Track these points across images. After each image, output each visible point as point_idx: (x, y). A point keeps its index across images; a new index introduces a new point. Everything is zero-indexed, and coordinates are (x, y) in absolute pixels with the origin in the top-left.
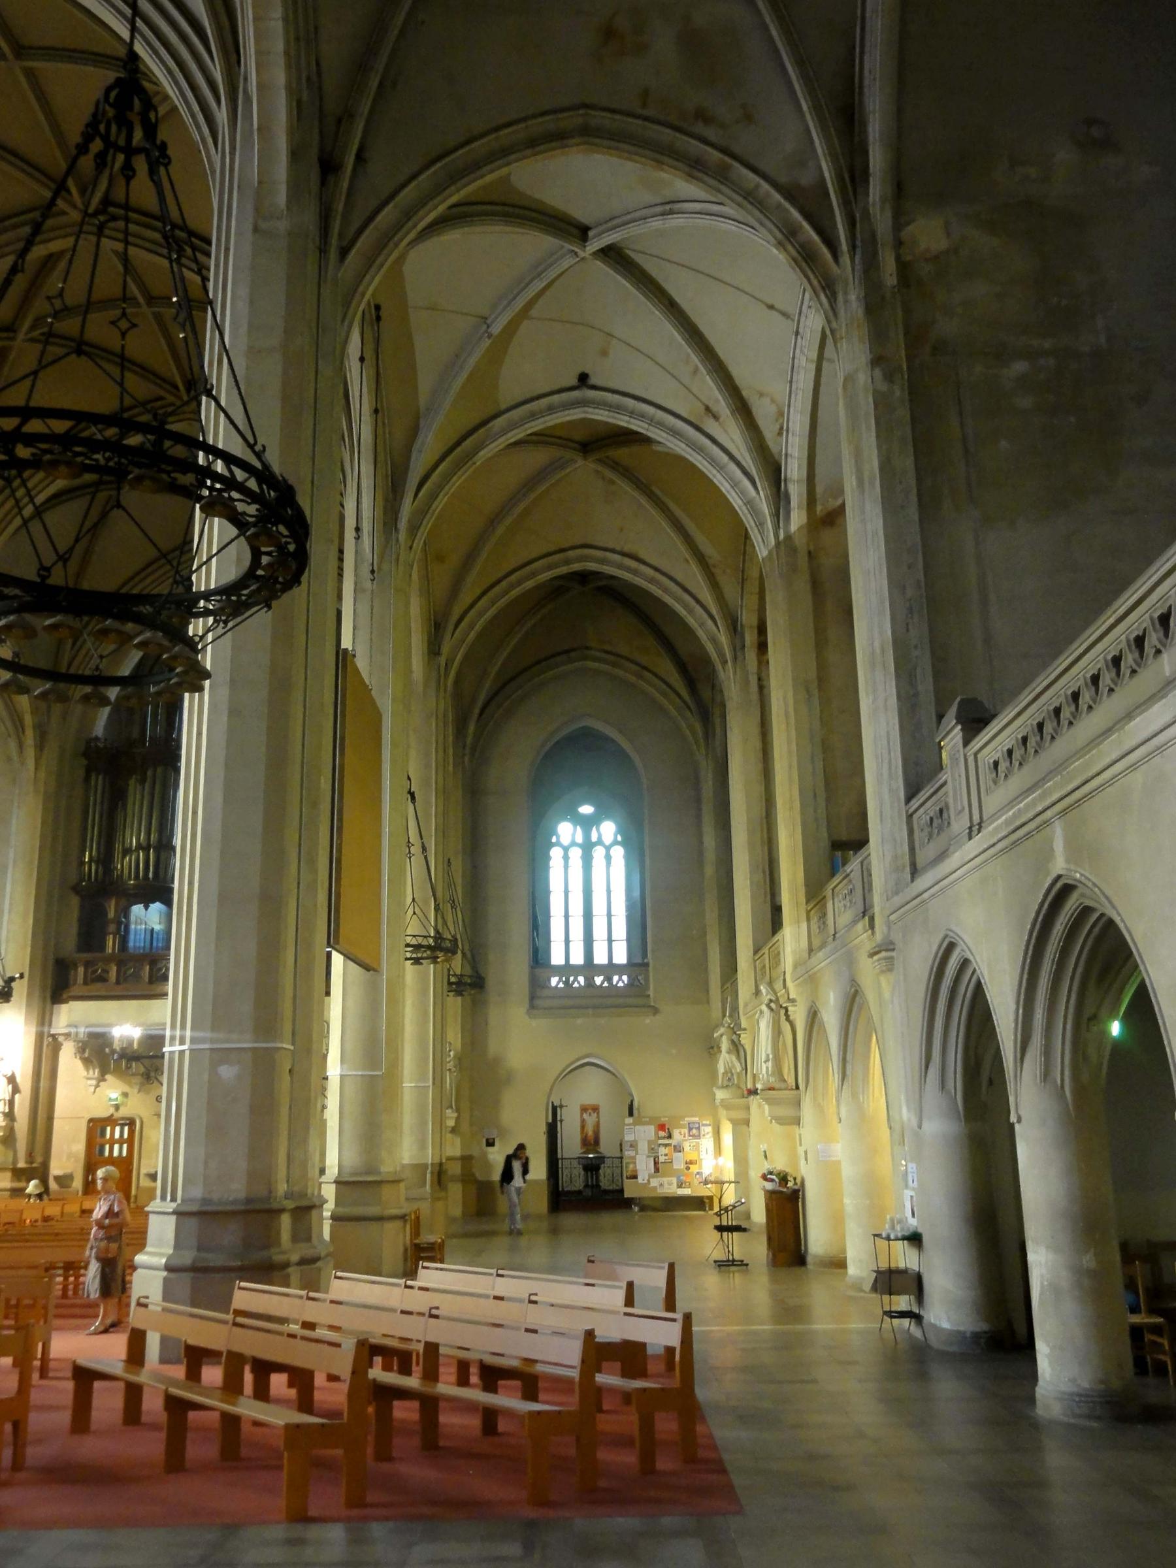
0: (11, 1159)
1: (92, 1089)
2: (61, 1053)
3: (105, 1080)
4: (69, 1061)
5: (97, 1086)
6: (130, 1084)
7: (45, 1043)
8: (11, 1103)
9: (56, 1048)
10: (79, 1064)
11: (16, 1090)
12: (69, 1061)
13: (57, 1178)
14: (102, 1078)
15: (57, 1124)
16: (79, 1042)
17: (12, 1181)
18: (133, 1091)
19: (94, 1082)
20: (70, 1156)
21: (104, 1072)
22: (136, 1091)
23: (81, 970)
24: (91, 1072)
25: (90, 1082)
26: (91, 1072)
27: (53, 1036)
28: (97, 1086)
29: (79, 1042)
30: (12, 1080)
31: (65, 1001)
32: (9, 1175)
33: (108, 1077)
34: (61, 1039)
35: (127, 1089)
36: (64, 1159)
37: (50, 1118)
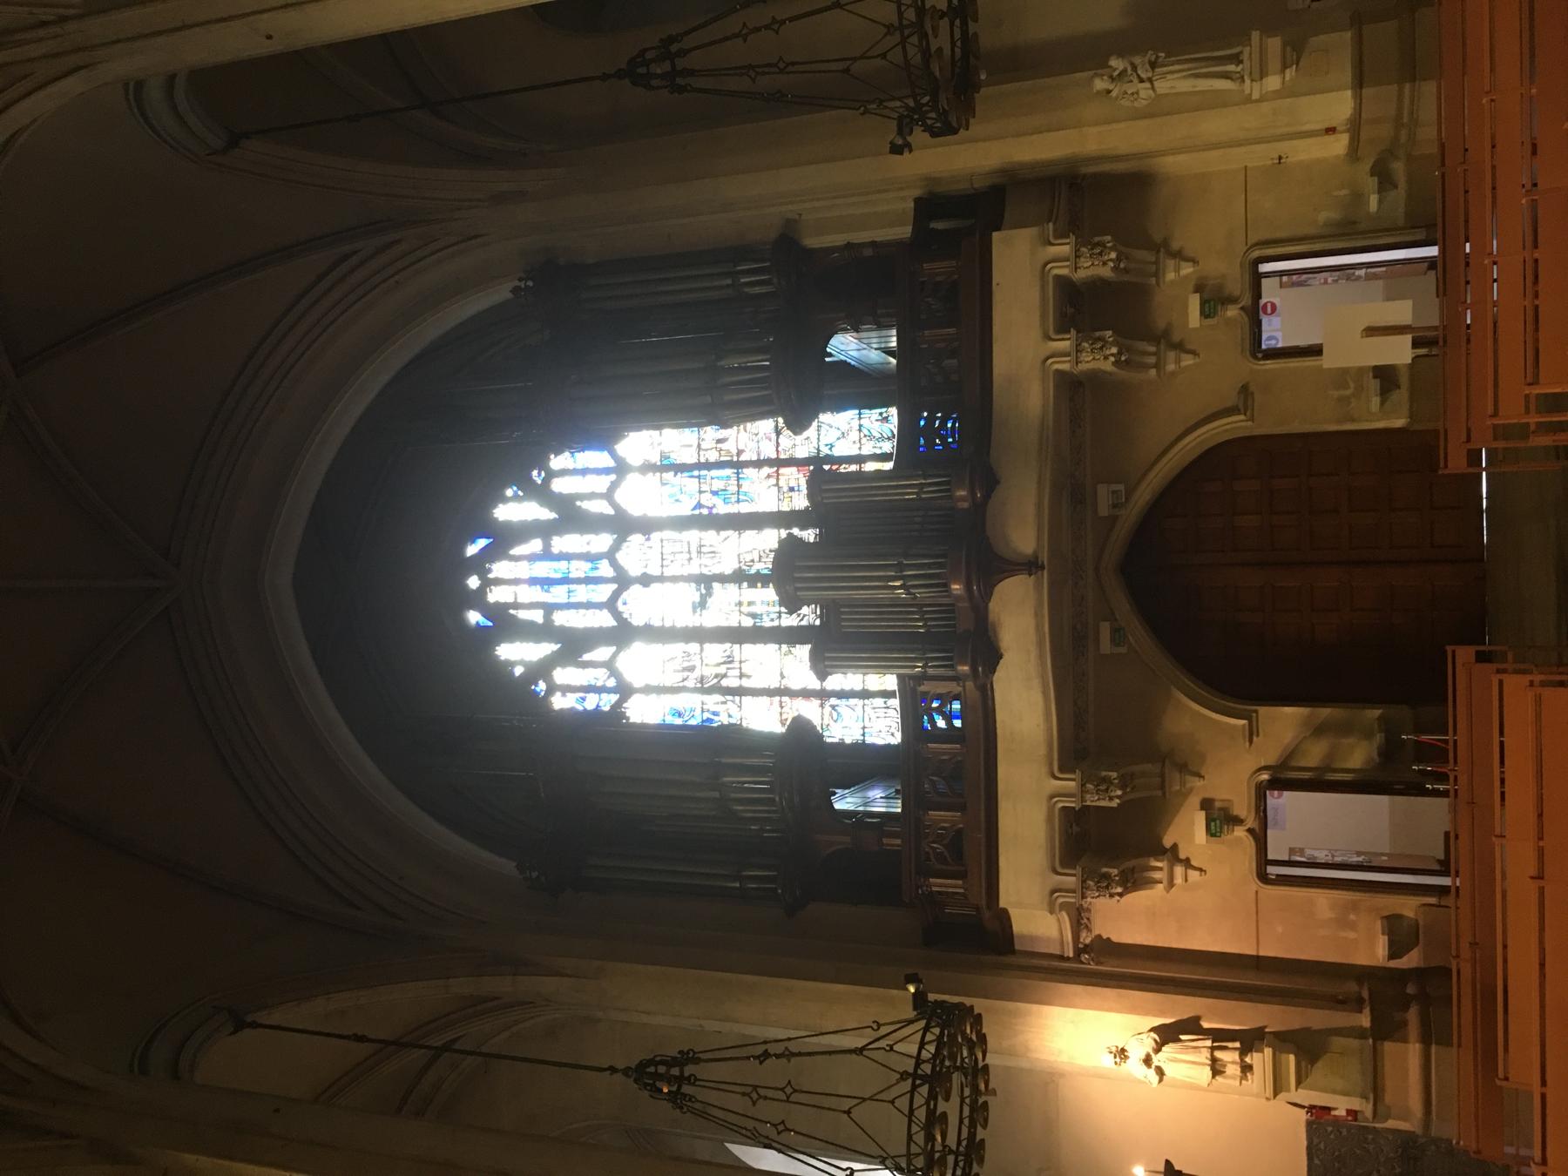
0: (1354, 1043)
1: (1194, 875)
2: (1115, 939)
3: (1175, 847)
4: (1129, 918)
5: (1187, 863)
6: (1185, 794)
7: (1093, 966)
8: (1219, 1036)
9: (1106, 948)
10: (1139, 899)
11: (1191, 1026)
12: (1129, 918)
13: (1393, 955)
14: (1173, 855)
15: (1270, 949)
16: (1084, 887)
17: (1405, 1040)
18: (1200, 788)
19: (1179, 870)
20: (1342, 923)
21: (1160, 851)
22: (1198, 783)
23: (937, 884)
24: (1157, 875)
25: (1179, 880)
26: (1157, 875)
27: (1079, 952)
28: (1187, 863)
29: (1084, 887)
30: (1167, 1035)
31: (1004, 917)
32: (1389, 1047)
33: (1168, 842)
34: (1086, 938)
35: (1195, 801)
36: (1352, 935)
37: (1258, 963)
